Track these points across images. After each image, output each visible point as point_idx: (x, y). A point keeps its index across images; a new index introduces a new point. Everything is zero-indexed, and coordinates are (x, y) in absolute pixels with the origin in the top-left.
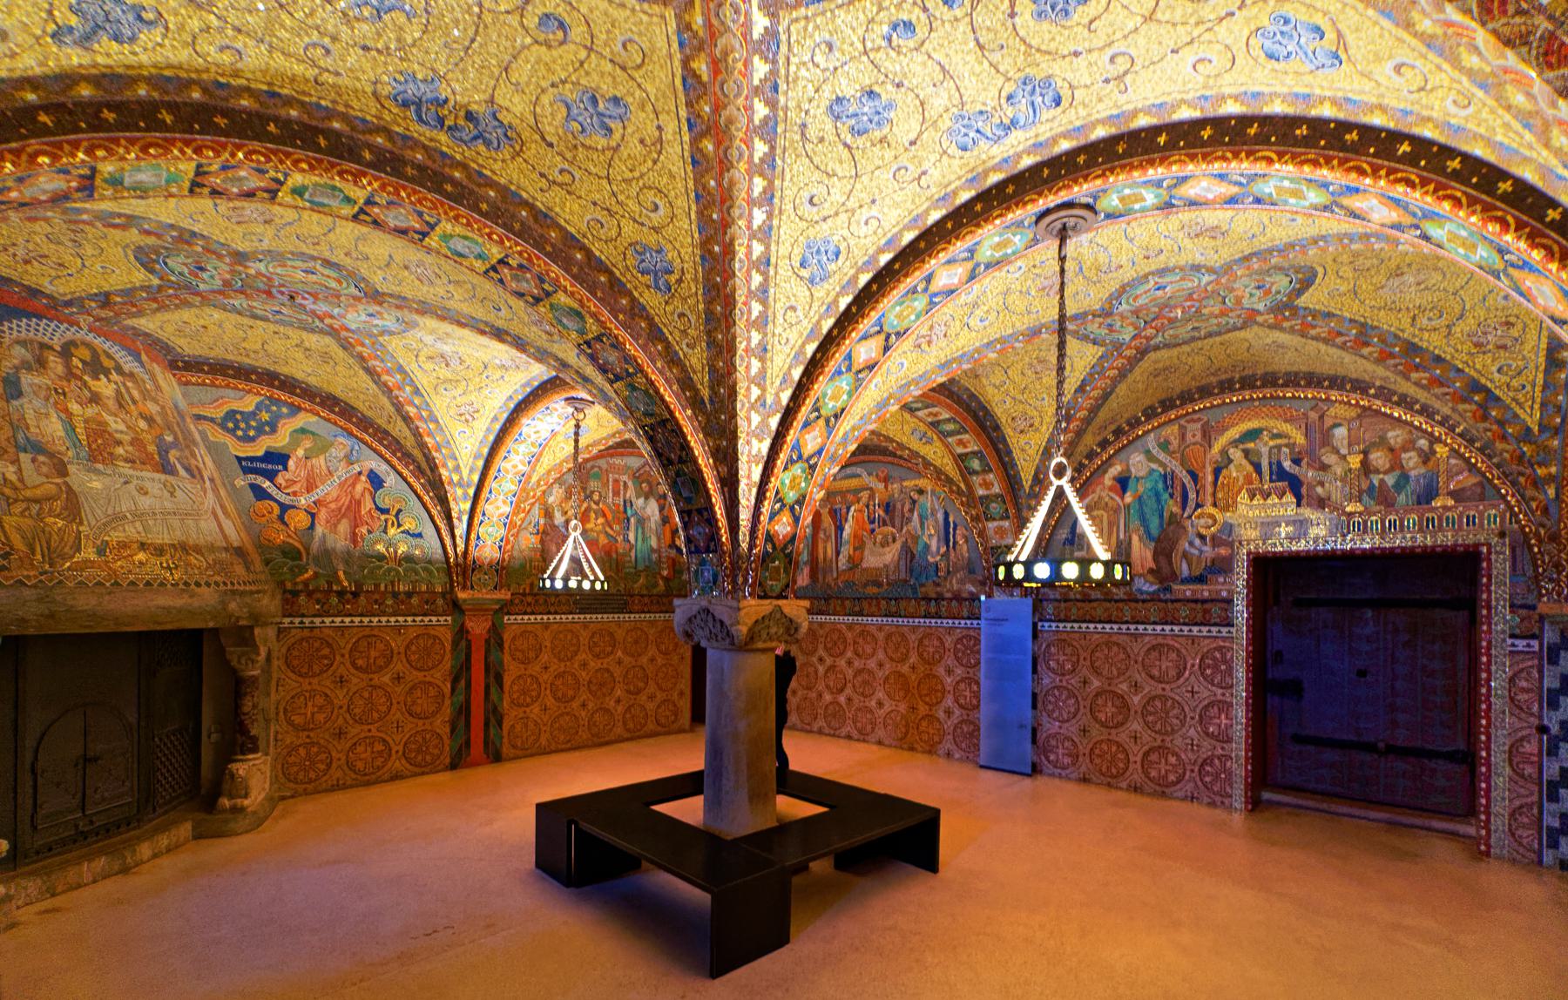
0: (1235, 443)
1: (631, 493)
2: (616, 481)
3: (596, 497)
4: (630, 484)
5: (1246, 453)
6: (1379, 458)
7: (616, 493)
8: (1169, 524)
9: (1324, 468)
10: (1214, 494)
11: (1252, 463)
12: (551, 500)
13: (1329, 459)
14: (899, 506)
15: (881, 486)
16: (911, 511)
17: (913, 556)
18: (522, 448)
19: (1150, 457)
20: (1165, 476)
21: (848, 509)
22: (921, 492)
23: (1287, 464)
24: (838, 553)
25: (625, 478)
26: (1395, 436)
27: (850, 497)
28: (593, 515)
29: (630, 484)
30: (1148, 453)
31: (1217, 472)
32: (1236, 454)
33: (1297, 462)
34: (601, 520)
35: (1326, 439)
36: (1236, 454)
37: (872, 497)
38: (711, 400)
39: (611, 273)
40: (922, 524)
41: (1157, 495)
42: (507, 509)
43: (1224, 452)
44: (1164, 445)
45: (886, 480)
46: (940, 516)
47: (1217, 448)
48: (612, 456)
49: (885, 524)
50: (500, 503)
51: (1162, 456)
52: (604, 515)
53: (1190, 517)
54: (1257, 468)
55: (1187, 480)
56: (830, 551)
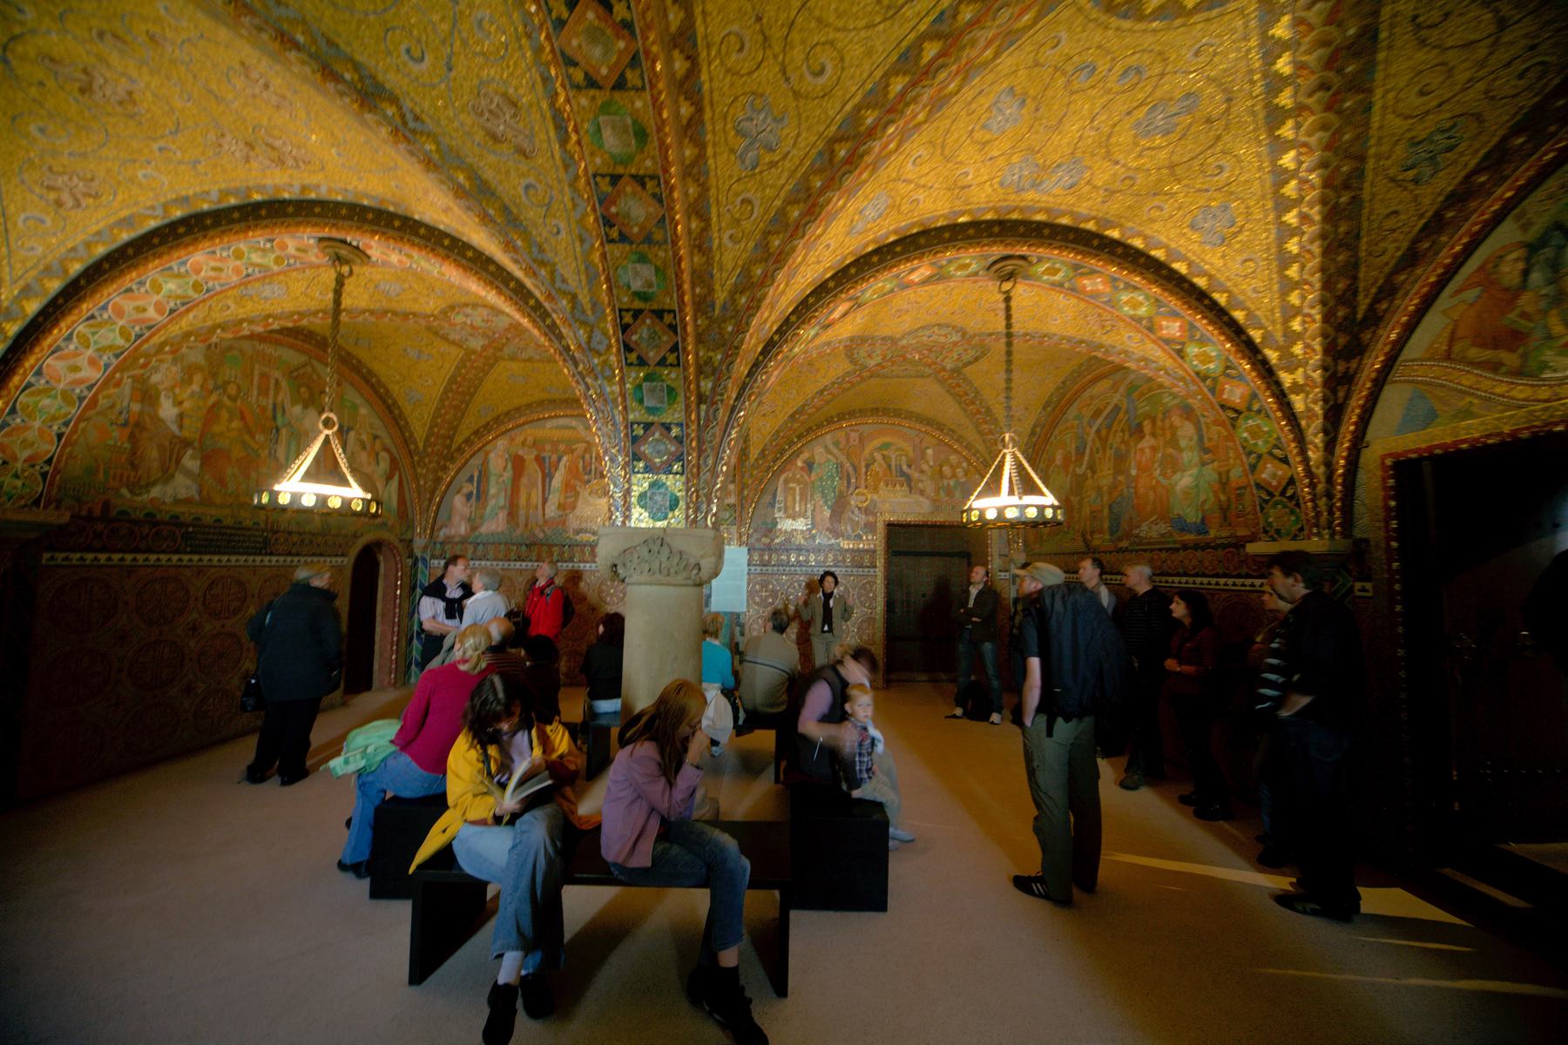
0: (879, 449)
1: (284, 396)
2: (264, 376)
3: (232, 390)
4: (284, 384)
5: (884, 457)
6: (946, 470)
7: (263, 391)
9: (922, 472)
12: (155, 378)
13: (925, 467)
18: (170, 286)
19: (828, 451)
21: (560, 459)
23: (905, 467)
24: (545, 501)
25: (277, 374)
26: (953, 458)
27: (562, 447)
28: (225, 415)
29: (284, 384)
30: (826, 447)
31: (867, 466)
32: (878, 456)
34: (236, 424)
36: (878, 456)
38: (724, 307)
39: (700, 110)
42: (90, 374)
43: (871, 454)
44: (836, 444)
47: (867, 451)
48: (278, 343)
50: (82, 361)
51: (835, 451)
52: (243, 418)
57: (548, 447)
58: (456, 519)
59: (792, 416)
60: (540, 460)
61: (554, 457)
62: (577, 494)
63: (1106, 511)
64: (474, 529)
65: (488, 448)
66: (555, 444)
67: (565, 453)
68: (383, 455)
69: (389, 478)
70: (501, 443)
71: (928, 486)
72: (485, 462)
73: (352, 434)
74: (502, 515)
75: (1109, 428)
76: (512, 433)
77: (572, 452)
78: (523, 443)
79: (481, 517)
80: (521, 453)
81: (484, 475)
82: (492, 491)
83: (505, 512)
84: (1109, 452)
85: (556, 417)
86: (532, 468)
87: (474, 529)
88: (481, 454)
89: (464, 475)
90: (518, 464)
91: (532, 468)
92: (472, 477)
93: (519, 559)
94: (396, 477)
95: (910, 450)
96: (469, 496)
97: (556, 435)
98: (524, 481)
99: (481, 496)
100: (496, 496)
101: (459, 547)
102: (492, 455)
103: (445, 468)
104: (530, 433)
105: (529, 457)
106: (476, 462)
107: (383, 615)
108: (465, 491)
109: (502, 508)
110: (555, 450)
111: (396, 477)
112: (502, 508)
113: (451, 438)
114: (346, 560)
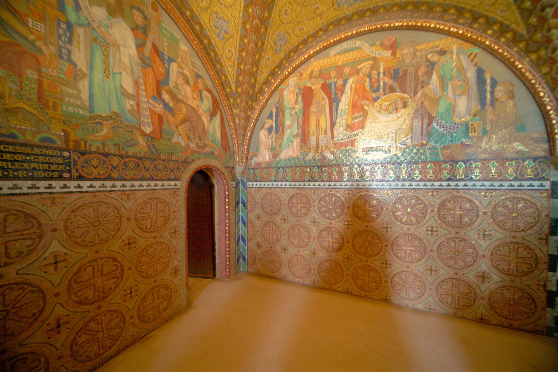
14: (411, 70)
15: (388, 53)
16: (429, 74)
17: (431, 119)
21: (345, 82)
22: (442, 53)
24: (333, 125)
27: (347, 70)
37: (375, 67)
40: (443, 86)
45: (393, 47)
46: (471, 74)
49: (392, 90)
56: (324, 122)
57: (333, 74)
58: (262, 149)
60: (326, 88)
61: (340, 82)
62: (365, 113)
64: (275, 156)
65: (282, 87)
66: (339, 69)
67: (350, 75)
68: (205, 93)
69: (213, 115)
70: (292, 81)
72: (281, 99)
73: (174, 66)
74: (296, 142)
76: (300, 69)
77: (358, 72)
78: (311, 76)
79: (280, 146)
80: (309, 85)
81: (280, 110)
82: (287, 123)
83: (299, 140)
85: (341, 41)
86: (320, 97)
87: (275, 156)
88: (277, 93)
89: (265, 113)
90: (307, 95)
91: (320, 97)
92: (271, 114)
93: (312, 179)
94: (218, 115)
96: (270, 130)
97: (341, 60)
98: (313, 109)
99: (278, 129)
100: (291, 127)
101: (265, 171)
102: (285, 92)
103: (252, 109)
104: (316, 65)
105: (316, 86)
106: (274, 100)
107: (219, 224)
108: (267, 126)
109: (295, 136)
110: (340, 75)
111: (218, 115)
112: (295, 136)
113: (253, 75)
114: (178, 183)
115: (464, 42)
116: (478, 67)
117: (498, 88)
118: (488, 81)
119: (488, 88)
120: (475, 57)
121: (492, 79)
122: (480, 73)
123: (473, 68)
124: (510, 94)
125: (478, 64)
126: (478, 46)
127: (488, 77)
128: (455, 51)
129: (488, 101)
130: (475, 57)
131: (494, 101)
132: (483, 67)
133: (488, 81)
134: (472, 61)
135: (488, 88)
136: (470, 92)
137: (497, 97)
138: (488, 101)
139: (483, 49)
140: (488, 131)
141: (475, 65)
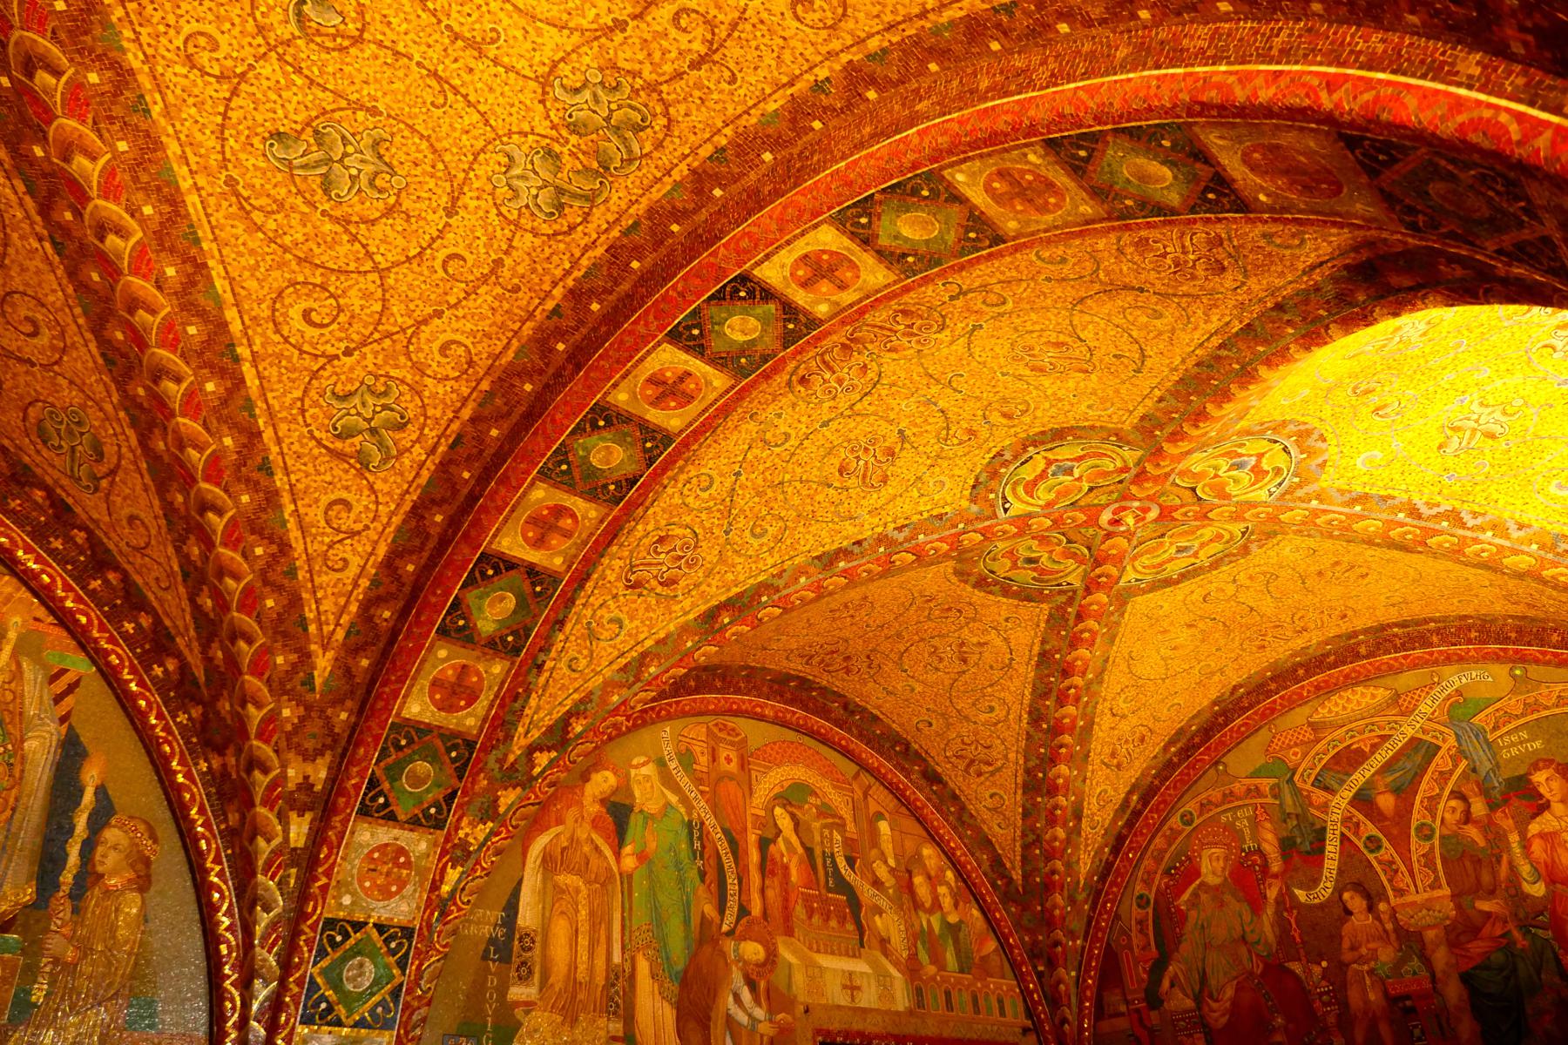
8: (701, 943)
10: (763, 891)
11: (802, 844)
13: (882, 872)
20: (690, 825)
23: (842, 863)
33: (851, 862)
35: (874, 834)
41: (678, 864)
46: (40, 746)
51: (684, 781)
53: (730, 933)
54: (809, 851)
55: (723, 847)
59: (711, 616)
63: (1453, 992)
71: (889, 924)
75: (1405, 793)
84: (1417, 847)
95: (846, 813)
115: (50, 619)
116: (71, 728)
117: (112, 835)
118: (88, 797)
119: (81, 822)
120: (71, 688)
121: (101, 791)
122: (71, 753)
123: (53, 727)
124: (140, 866)
125: (73, 720)
126: (88, 654)
127: (91, 776)
128: (12, 635)
129: (67, 877)
130: (71, 688)
131: (88, 876)
132: (86, 737)
133: (88, 797)
134: (58, 699)
135: (81, 822)
136: (17, 816)
137: (100, 869)
138: (67, 877)
139: (100, 670)
140: (35, 1005)
141: (63, 720)
